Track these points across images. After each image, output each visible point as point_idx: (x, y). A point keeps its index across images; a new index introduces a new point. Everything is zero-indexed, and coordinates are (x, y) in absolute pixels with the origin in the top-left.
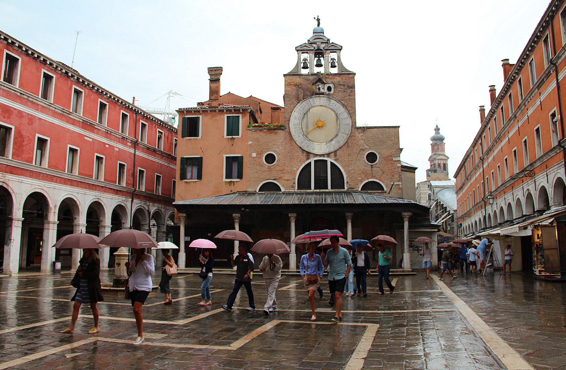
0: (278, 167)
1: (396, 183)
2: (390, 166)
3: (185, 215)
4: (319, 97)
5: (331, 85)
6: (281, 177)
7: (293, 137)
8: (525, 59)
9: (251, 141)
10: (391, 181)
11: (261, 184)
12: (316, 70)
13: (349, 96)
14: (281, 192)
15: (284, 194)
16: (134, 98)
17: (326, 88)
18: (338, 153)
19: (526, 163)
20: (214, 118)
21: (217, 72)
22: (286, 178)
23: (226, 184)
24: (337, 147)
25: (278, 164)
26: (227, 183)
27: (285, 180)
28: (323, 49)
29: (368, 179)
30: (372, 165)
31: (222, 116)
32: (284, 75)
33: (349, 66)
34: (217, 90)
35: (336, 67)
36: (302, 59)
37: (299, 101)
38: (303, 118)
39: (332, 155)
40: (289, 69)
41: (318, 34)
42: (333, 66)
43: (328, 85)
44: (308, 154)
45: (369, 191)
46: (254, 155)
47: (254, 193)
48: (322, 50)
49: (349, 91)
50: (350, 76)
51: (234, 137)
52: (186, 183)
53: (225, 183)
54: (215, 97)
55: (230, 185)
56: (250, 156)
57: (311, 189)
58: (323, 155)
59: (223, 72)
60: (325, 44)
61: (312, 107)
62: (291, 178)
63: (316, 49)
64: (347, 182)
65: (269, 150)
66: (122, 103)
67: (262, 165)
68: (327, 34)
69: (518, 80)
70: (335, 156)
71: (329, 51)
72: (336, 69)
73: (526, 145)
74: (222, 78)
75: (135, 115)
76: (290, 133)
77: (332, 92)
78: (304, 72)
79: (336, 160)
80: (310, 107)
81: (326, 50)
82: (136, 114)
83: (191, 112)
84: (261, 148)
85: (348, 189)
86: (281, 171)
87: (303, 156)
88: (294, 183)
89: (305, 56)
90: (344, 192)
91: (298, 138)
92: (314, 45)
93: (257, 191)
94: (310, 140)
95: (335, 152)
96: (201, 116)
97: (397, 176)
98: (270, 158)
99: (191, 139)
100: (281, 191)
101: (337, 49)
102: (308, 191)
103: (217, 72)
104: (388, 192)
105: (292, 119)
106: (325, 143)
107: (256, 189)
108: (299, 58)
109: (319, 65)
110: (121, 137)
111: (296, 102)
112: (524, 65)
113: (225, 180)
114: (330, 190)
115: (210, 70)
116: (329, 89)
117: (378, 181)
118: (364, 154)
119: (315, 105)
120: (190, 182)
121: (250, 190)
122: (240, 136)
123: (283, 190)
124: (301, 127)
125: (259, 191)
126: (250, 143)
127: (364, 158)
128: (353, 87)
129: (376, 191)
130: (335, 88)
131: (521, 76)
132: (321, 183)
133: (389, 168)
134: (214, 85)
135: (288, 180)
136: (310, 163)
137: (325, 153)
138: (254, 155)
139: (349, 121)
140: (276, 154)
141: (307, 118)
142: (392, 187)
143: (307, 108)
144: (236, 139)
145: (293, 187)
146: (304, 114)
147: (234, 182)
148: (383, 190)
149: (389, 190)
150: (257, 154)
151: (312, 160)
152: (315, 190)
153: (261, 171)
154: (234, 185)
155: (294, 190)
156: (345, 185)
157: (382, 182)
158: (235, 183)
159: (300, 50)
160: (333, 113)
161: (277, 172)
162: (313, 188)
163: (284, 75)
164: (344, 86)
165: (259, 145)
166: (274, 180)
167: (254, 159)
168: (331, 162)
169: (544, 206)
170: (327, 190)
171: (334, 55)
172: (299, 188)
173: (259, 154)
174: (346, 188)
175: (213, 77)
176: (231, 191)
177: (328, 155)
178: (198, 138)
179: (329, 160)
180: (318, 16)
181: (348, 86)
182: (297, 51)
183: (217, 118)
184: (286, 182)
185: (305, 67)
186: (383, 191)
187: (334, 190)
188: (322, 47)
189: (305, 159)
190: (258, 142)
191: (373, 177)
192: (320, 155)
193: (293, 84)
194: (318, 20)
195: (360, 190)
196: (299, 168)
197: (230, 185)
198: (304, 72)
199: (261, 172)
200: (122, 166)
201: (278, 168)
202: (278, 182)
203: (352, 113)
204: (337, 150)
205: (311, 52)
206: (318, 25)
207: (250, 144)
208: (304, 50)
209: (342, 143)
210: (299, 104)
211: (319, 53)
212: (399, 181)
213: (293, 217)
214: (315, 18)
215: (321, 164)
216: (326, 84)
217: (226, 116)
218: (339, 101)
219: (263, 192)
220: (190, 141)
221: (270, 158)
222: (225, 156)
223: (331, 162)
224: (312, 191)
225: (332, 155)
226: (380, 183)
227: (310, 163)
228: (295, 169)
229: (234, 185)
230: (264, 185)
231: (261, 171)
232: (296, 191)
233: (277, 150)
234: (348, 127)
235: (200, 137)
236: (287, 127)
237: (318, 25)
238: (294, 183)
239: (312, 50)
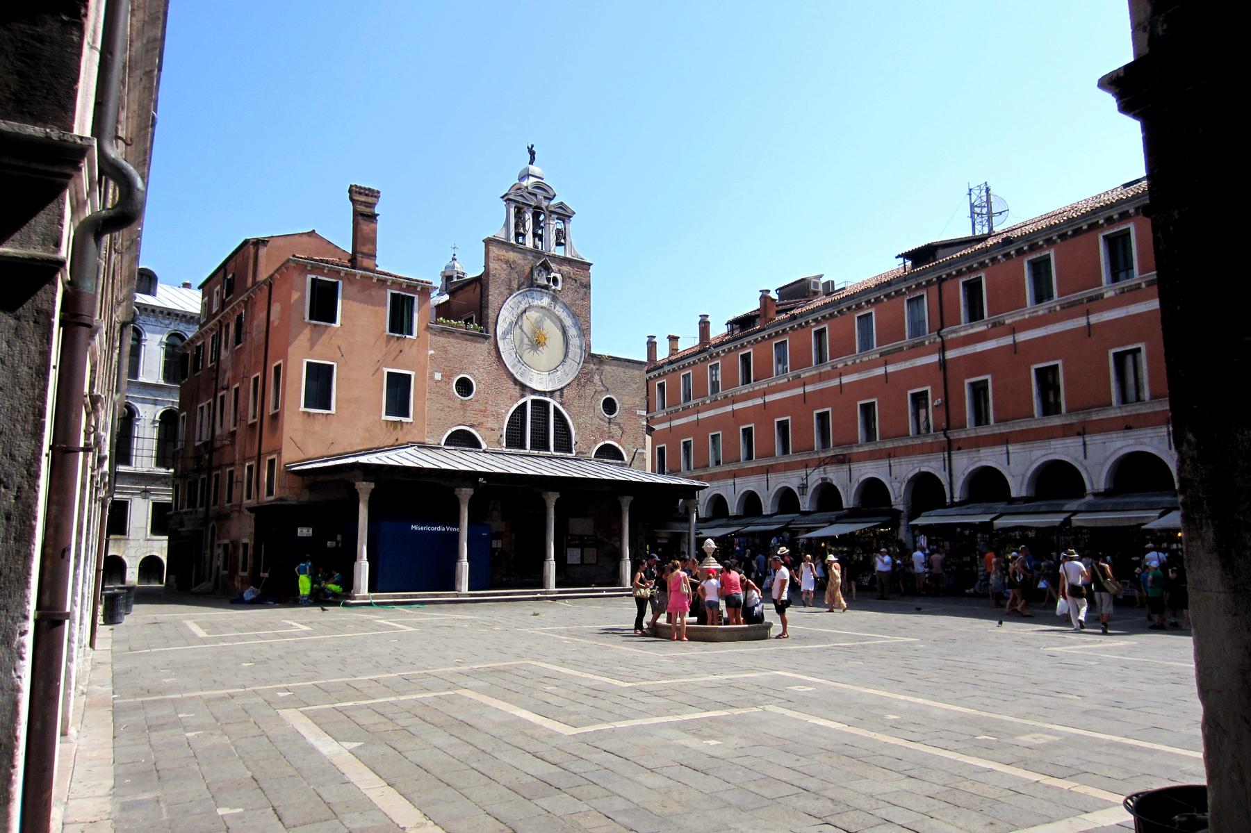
0: (476, 403)
1: (639, 451)
2: (632, 423)
3: (372, 486)
4: (541, 291)
5: (559, 276)
6: (482, 423)
7: (502, 353)
9: (434, 349)
10: (634, 448)
13: (582, 299)
14: (481, 450)
18: (565, 390)
20: (367, 292)
21: (370, 200)
22: (489, 425)
23: (387, 426)
25: (476, 398)
26: (389, 423)
27: (487, 429)
28: (545, 209)
30: (610, 419)
31: (382, 292)
34: (372, 235)
42: (559, 244)
44: (523, 387)
45: (605, 460)
46: (438, 376)
48: (542, 209)
49: (582, 291)
50: (585, 266)
52: (306, 415)
53: (385, 422)
54: (369, 249)
55: (395, 428)
56: (432, 377)
57: (525, 449)
58: (544, 393)
60: (548, 201)
62: (496, 426)
64: (576, 443)
65: (462, 370)
67: (451, 398)
70: (561, 396)
71: (556, 216)
79: (561, 404)
80: (527, 306)
81: (552, 212)
84: (449, 365)
86: (481, 411)
87: (516, 391)
88: (501, 436)
93: (443, 443)
95: (561, 390)
97: (641, 440)
98: (465, 387)
100: (479, 446)
101: (564, 215)
102: (522, 451)
103: (370, 200)
104: (629, 463)
106: (547, 373)
107: (441, 440)
111: (506, 292)
113: (384, 417)
115: (354, 191)
117: (616, 445)
120: (315, 414)
121: (430, 441)
122: (414, 337)
123: (484, 446)
126: (431, 352)
127: (600, 405)
128: (587, 286)
129: (615, 461)
130: (563, 281)
133: (631, 425)
136: (525, 404)
137: (547, 390)
142: (634, 456)
143: (523, 307)
144: (406, 341)
145: (499, 443)
148: (622, 459)
149: (630, 461)
151: (529, 398)
152: (532, 452)
153: (449, 407)
154: (401, 429)
157: (623, 447)
158: (404, 424)
161: (475, 413)
162: (529, 448)
164: (576, 281)
165: (446, 359)
166: (472, 426)
167: (438, 384)
168: (555, 407)
169: (859, 503)
170: (549, 453)
172: (508, 446)
173: (447, 377)
174: (574, 451)
176: (397, 440)
178: (333, 325)
179: (553, 403)
180: (532, 146)
181: (581, 284)
183: (373, 293)
184: (488, 433)
186: (623, 462)
187: (558, 454)
188: (545, 204)
189: (518, 395)
190: (446, 351)
191: (611, 438)
193: (502, 258)
194: (532, 153)
195: (593, 456)
196: (509, 410)
197: (395, 428)
199: (448, 409)
201: (477, 406)
202: (477, 431)
203: (584, 332)
204: (565, 387)
207: (431, 355)
210: (512, 297)
213: (626, 502)
217: (389, 292)
218: (566, 307)
220: (317, 329)
221: (465, 387)
222: (386, 370)
223: (555, 407)
224: (527, 451)
226: (620, 448)
227: (525, 404)
228: (503, 411)
229: (401, 429)
230: (453, 433)
231: (449, 407)
238: (501, 436)
239: (530, 206)
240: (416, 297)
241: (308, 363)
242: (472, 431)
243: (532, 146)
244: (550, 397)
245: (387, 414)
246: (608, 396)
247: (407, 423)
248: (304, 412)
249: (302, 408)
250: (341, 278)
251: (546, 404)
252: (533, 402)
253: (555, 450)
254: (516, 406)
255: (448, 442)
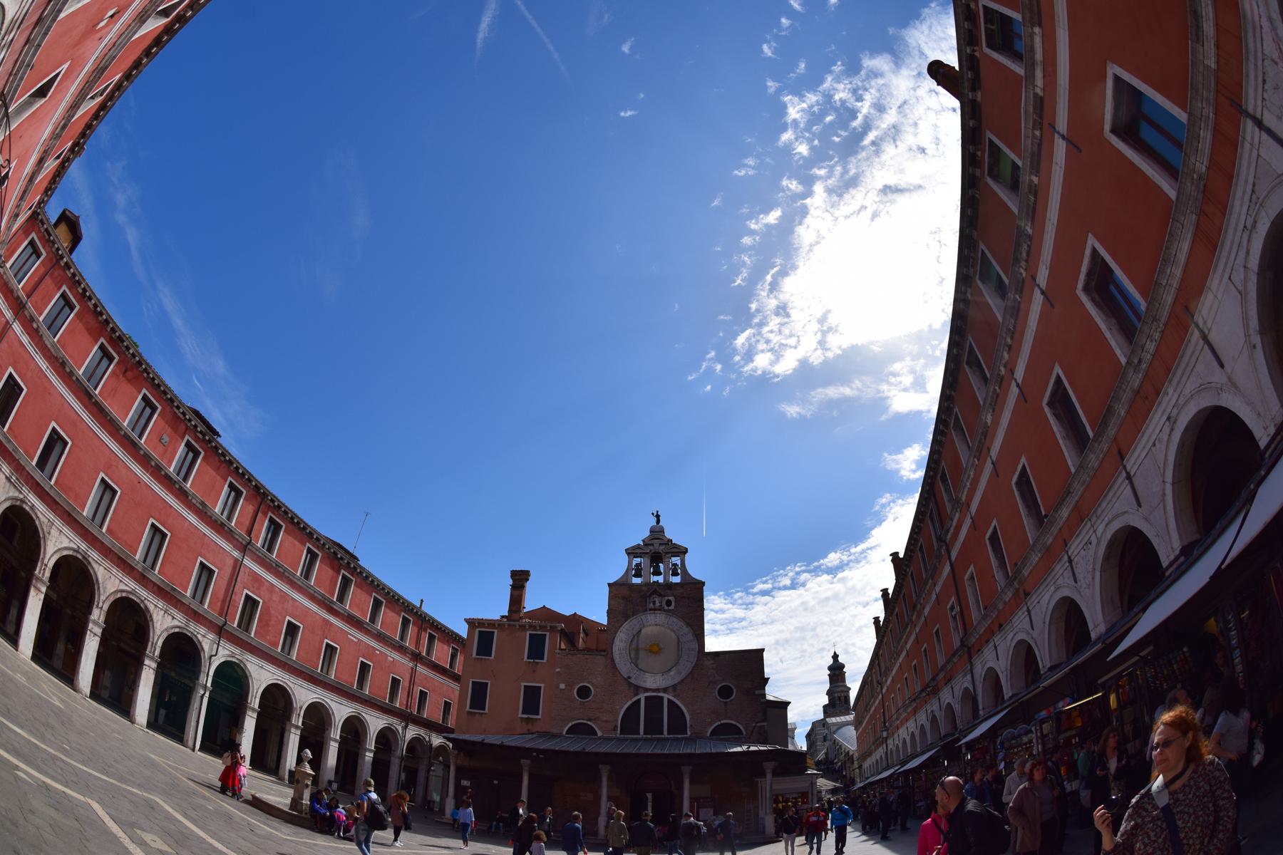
8: (913, 545)
11: (570, 725)
12: (654, 579)
15: (600, 738)
16: (422, 601)
17: (665, 602)
19: (928, 676)
22: (605, 719)
24: (677, 680)
29: (720, 721)
30: (726, 703)
32: (609, 585)
33: (695, 571)
35: (678, 574)
36: (634, 564)
37: (626, 618)
38: (632, 641)
39: (670, 690)
40: (617, 573)
41: (657, 532)
42: (675, 574)
43: (666, 598)
44: (637, 689)
45: (722, 737)
46: (562, 686)
47: (559, 735)
48: (660, 553)
51: (537, 661)
56: (557, 687)
58: (657, 690)
59: (530, 578)
61: (644, 626)
63: (653, 551)
66: (403, 603)
68: (668, 535)
69: (910, 573)
71: (670, 555)
72: (679, 577)
73: (926, 655)
74: (528, 585)
75: (420, 622)
76: (613, 660)
77: (672, 607)
78: (637, 581)
79: (675, 696)
82: (422, 621)
83: (484, 624)
85: (692, 734)
89: (637, 560)
90: (686, 739)
91: (624, 667)
92: (651, 547)
93: (564, 733)
94: (641, 670)
95: (674, 687)
96: (496, 631)
98: (584, 692)
99: (481, 659)
101: (682, 552)
105: (617, 641)
107: (563, 730)
108: (630, 563)
109: (657, 573)
110: (398, 645)
112: (914, 553)
114: (667, 736)
116: (669, 603)
118: (715, 689)
119: (648, 624)
121: (555, 731)
123: (600, 734)
124: (628, 652)
125: (567, 733)
126: (558, 670)
127: (715, 692)
130: (676, 602)
131: (912, 568)
132: (654, 725)
134: (516, 593)
135: (607, 721)
136: (639, 700)
138: (562, 686)
139: (695, 645)
140: (593, 686)
141: (638, 641)
143: (637, 628)
146: (634, 636)
147: (532, 719)
150: (566, 686)
151: (642, 696)
155: (616, 734)
156: (688, 729)
159: (632, 552)
160: (673, 634)
163: (609, 585)
168: (669, 700)
171: (676, 560)
173: (570, 686)
174: (689, 733)
175: (517, 582)
177: (665, 690)
179: (666, 696)
180: (657, 512)
182: (628, 554)
185: (638, 575)
187: (671, 736)
192: (654, 690)
194: (658, 516)
195: (708, 734)
198: (637, 581)
200: (395, 682)
205: (647, 556)
206: (658, 522)
208: (637, 553)
209: (684, 674)
211: (656, 559)
212: (764, 721)
214: (653, 514)
215: (653, 703)
216: (665, 596)
217: (528, 633)
219: (572, 736)
221: (584, 692)
222: (523, 684)
223: (669, 700)
225: (670, 690)
226: (738, 724)
227: (639, 700)
230: (572, 726)
232: (618, 736)
233: (594, 681)
234: (693, 652)
235: (492, 658)
236: (610, 653)
237: (658, 522)
239: (647, 553)
240: (548, 634)
241: (473, 682)
242: (589, 723)
243: (657, 512)
244: (664, 692)
245: (523, 713)
246: (723, 684)
247: (536, 719)
248: (469, 712)
249: (468, 708)
250: (496, 629)
251: (662, 698)
252: (646, 698)
253: (668, 734)
254: (629, 703)
255: (568, 732)
